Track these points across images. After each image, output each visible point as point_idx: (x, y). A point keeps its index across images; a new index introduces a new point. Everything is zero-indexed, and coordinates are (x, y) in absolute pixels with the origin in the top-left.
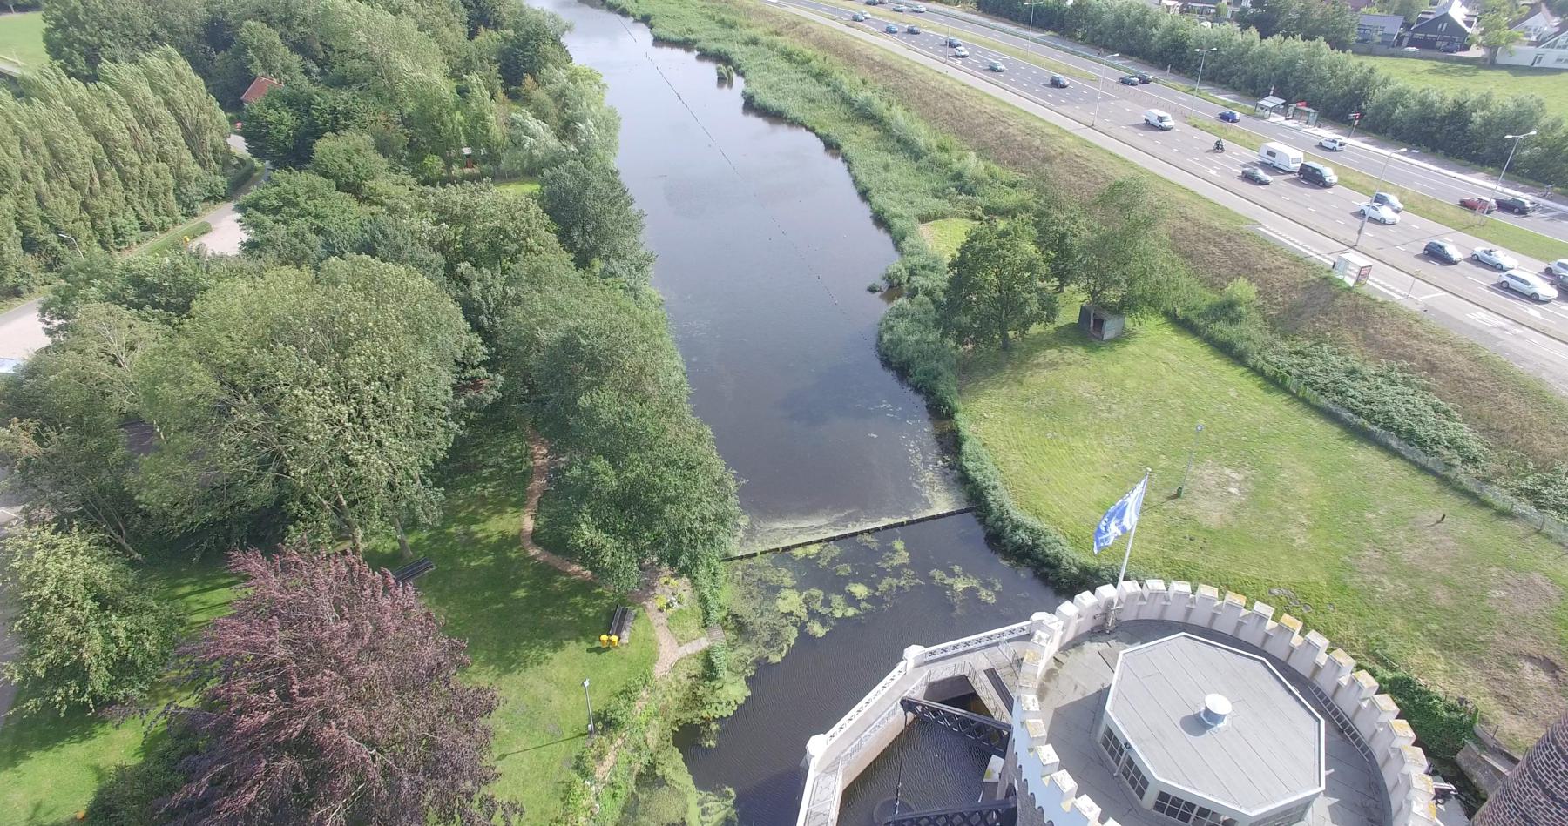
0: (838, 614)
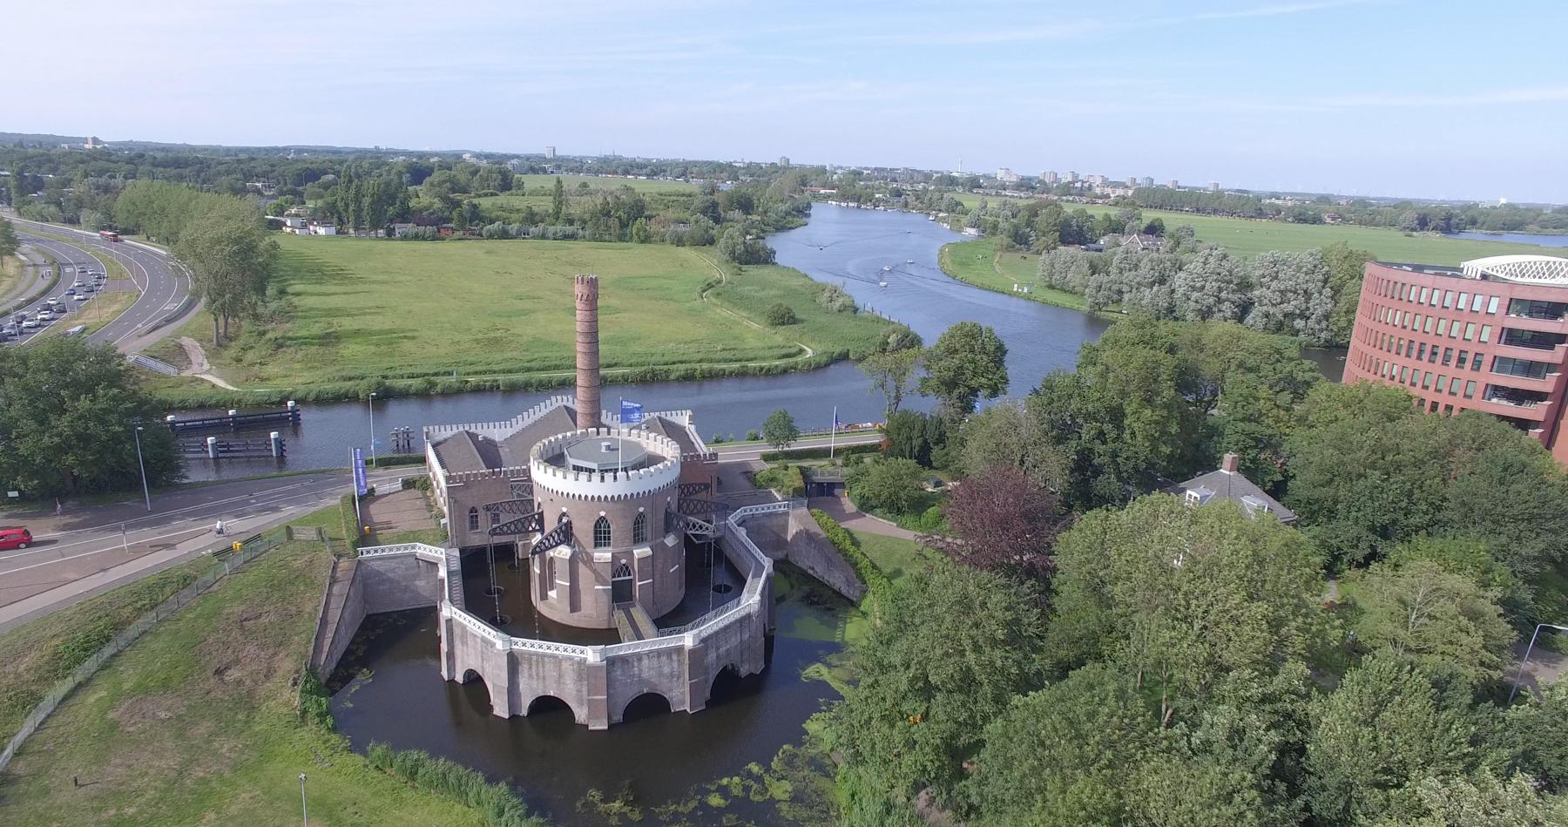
0: (736, 779)
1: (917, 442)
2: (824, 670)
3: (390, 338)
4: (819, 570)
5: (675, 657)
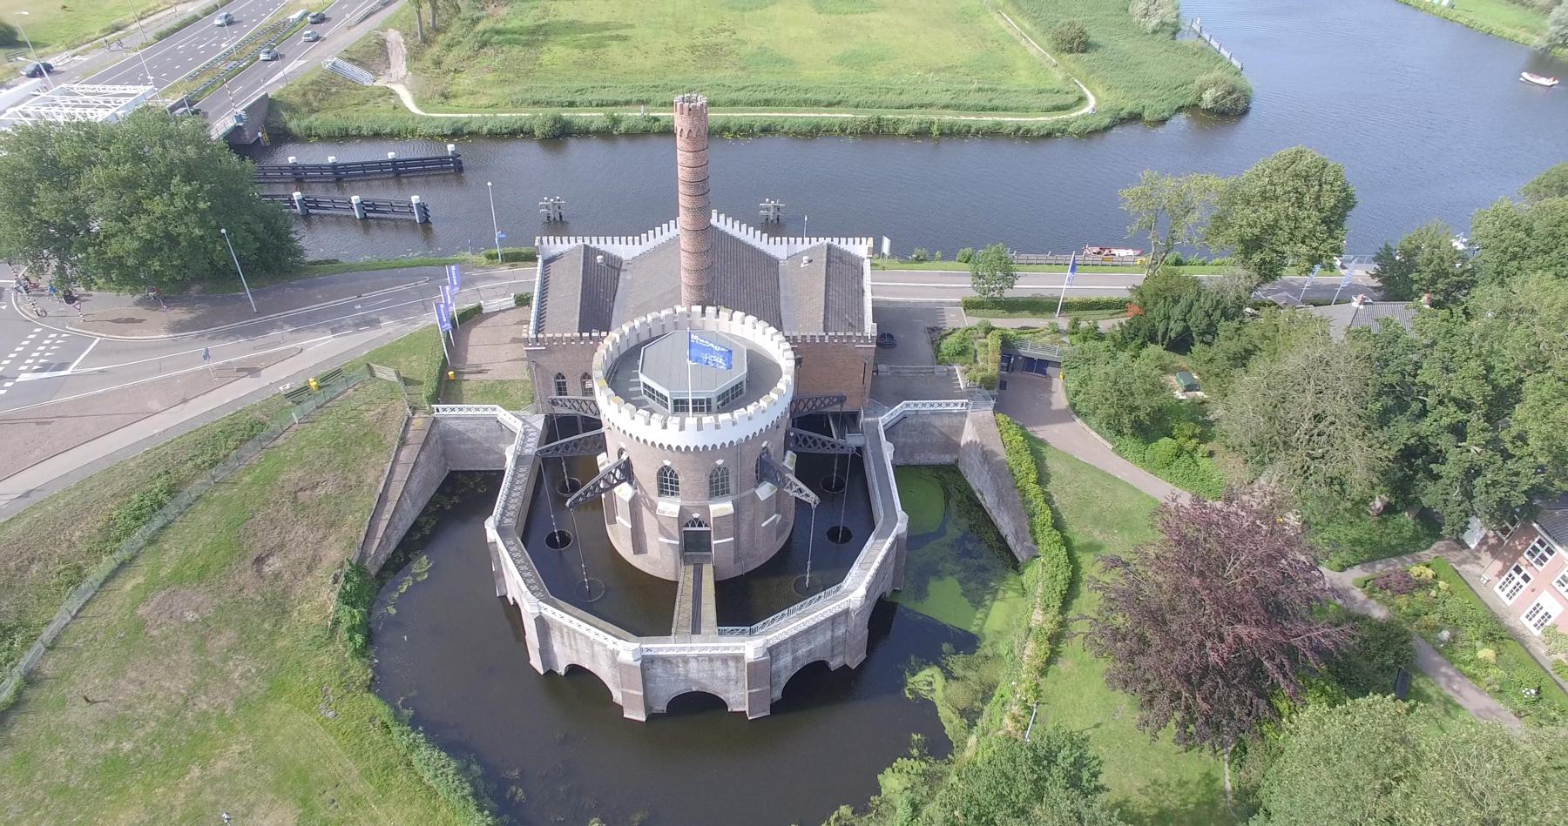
1: (1176, 328)
2: (939, 681)
3: (600, 35)
4: (989, 501)
5: (731, 664)
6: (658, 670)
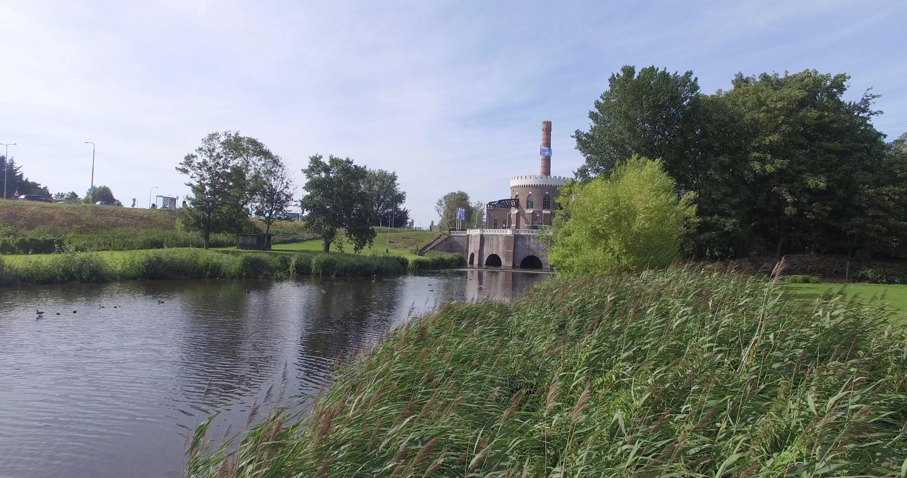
6: (520, 242)
